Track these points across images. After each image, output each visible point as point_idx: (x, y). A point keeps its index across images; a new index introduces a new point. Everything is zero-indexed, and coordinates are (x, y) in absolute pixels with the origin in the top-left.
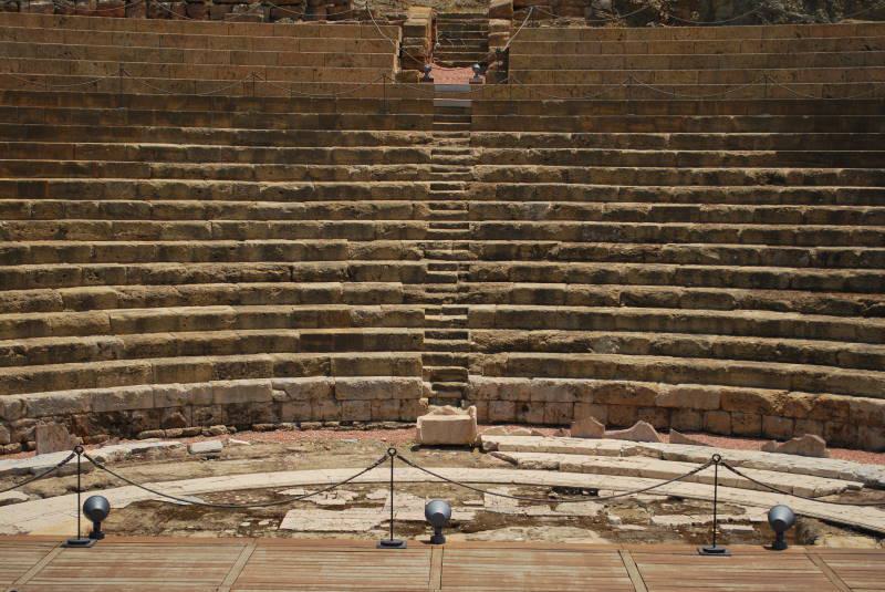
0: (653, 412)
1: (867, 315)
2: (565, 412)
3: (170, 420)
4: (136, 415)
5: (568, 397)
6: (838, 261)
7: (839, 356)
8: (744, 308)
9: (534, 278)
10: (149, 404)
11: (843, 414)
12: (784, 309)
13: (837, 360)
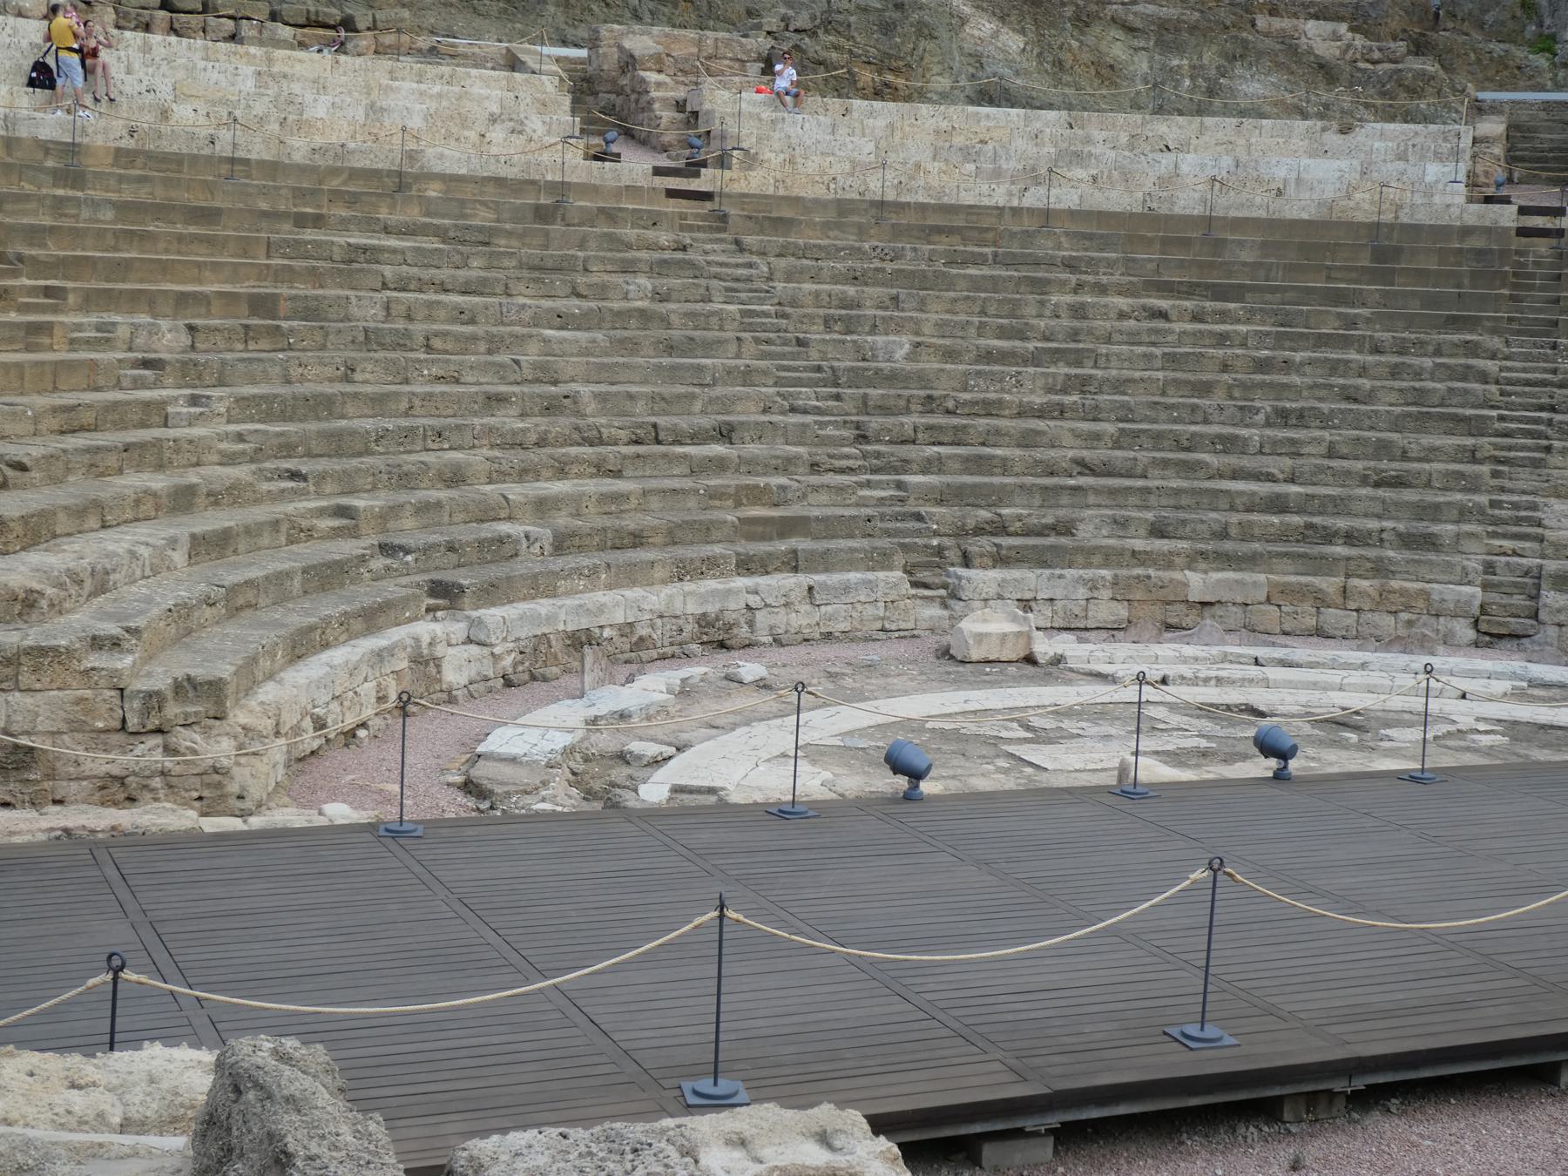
0: (1183, 607)
1: (1377, 485)
2: (1077, 611)
3: (641, 639)
4: (607, 633)
5: (1082, 592)
6: (1301, 418)
7: (1384, 535)
8: (1221, 477)
9: (946, 440)
10: (619, 617)
11: (1421, 604)
12: (1270, 478)
13: (1381, 540)
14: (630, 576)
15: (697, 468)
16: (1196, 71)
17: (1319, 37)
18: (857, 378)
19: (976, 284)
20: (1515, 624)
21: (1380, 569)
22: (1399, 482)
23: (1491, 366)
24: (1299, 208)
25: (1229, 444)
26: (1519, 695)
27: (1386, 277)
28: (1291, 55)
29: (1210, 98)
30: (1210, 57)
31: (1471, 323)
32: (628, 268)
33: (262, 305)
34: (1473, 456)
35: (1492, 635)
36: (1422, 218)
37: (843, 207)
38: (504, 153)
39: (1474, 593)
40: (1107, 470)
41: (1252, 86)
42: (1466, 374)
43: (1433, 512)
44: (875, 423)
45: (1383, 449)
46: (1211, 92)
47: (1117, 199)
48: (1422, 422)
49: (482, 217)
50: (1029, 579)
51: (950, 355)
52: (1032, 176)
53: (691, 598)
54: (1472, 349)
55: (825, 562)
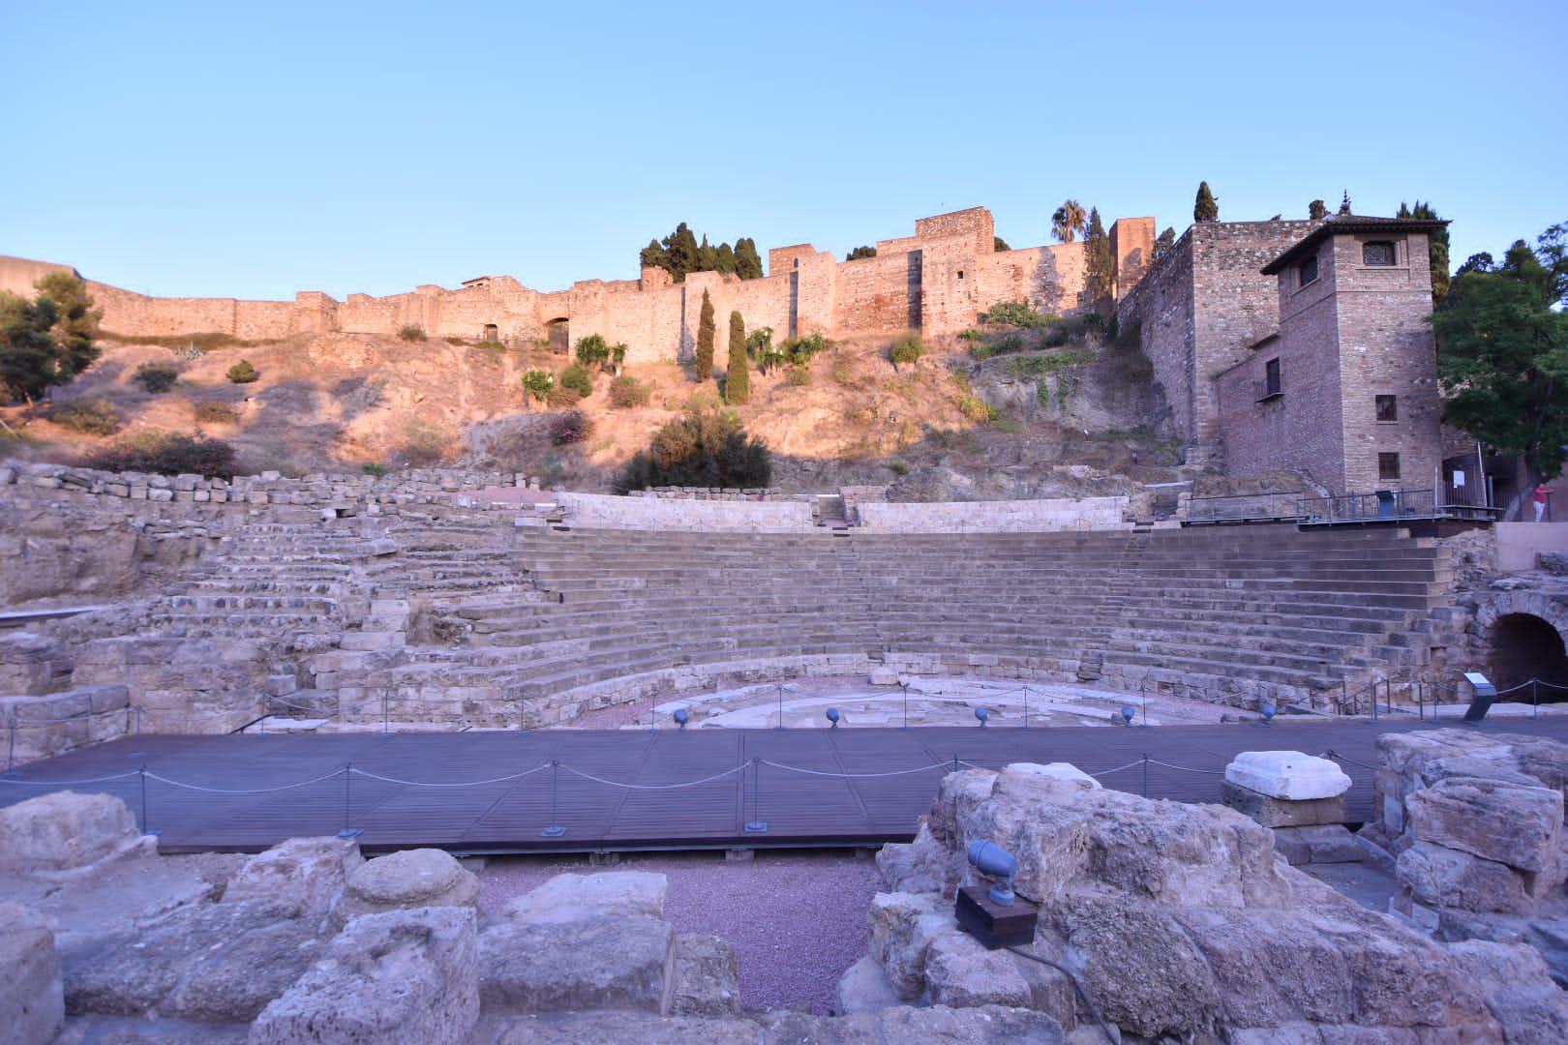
6: (1031, 600)
14: (762, 654)
15: (805, 620)
17: (1076, 470)
18: (876, 590)
20: (1093, 675)
21: (1041, 654)
23: (1108, 580)
24: (1055, 528)
25: (1002, 610)
26: (1077, 702)
28: (1063, 477)
29: (1035, 493)
30: (1034, 481)
31: (1106, 565)
32: (812, 558)
33: (678, 574)
34: (1091, 612)
35: (1085, 680)
36: (1099, 528)
37: (893, 536)
38: (786, 526)
39: (1078, 663)
41: (1048, 488)
43: (1069, 633)
47: (990, 530)
48: (1074, 600)
49: (770, 545)
50: (910, 656)
51: (912, 582)
52: (963, 522)
53: (783, 662)
54: (1103, 574)
55: (834, 651)
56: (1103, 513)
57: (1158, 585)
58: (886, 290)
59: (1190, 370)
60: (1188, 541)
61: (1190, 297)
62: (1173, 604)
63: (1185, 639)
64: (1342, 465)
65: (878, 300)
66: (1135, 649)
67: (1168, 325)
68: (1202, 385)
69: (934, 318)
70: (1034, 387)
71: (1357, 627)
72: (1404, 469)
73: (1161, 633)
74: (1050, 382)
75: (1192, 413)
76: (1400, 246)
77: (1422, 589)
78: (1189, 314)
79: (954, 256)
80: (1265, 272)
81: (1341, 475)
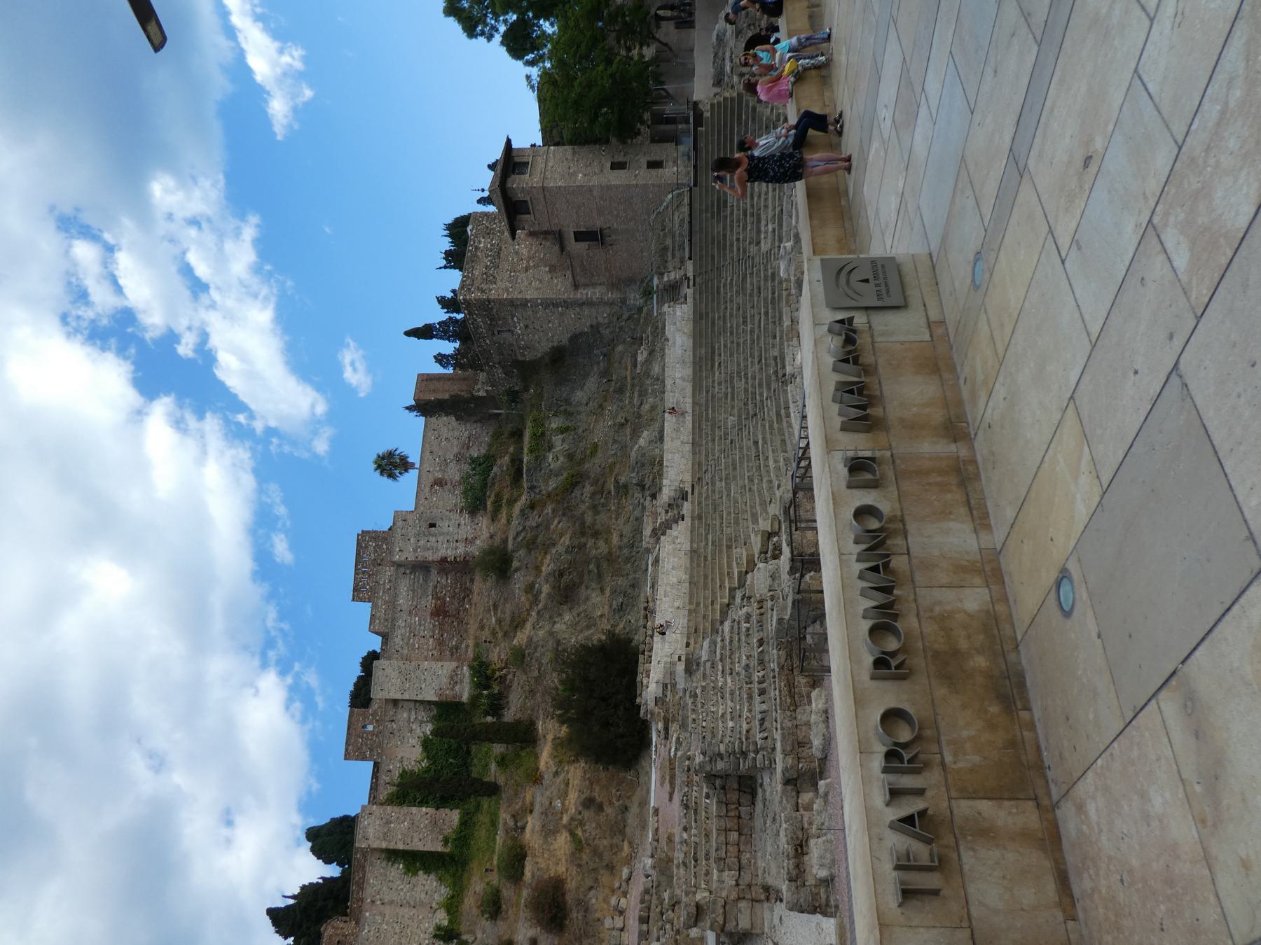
6: (745, 318)
16: (652, 385)
19: (713, 411)
21: (781, 283)
22: (759, 288)
27: (707, 314)
28: (648, 362)
29: (660, 380)
31: (718, 288)
40: (760, 356)
41: (656, 369)
42: (731, 283)
44: (751, 413)
45: (751, 295)
46: (658, 379)
48: (744, 289)
55: (787, 402)
56: (678, 322)
57: (732, 245)
58: (428, 602)
59: (567, 304)
60: (701, 257)
61: (512, 303)
62: (744, 229)
63: (766, 207)
64: (653, 185)
65: (440, 612)
66: (774, 230)
67: (527, 327)
68: (582, 294)
69: (469, 549)
70: (557, 440)
71: (754, 119)
72: (657, 158)
73: (763, 223)
74: (555, 424)
75: (602, 303)
76: (517, 160)
77: (732, 99)
78: (524, 304)
79: (412, 532)
80: (513, 237)
81: (659, 186)
